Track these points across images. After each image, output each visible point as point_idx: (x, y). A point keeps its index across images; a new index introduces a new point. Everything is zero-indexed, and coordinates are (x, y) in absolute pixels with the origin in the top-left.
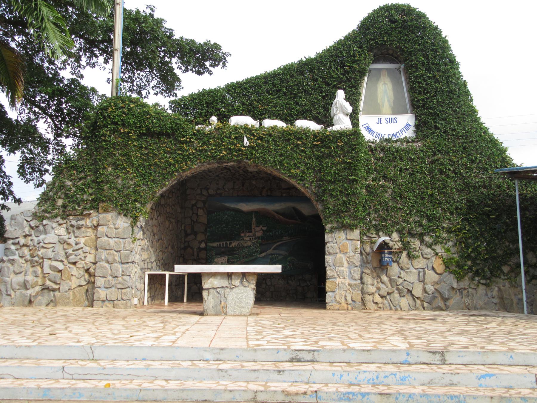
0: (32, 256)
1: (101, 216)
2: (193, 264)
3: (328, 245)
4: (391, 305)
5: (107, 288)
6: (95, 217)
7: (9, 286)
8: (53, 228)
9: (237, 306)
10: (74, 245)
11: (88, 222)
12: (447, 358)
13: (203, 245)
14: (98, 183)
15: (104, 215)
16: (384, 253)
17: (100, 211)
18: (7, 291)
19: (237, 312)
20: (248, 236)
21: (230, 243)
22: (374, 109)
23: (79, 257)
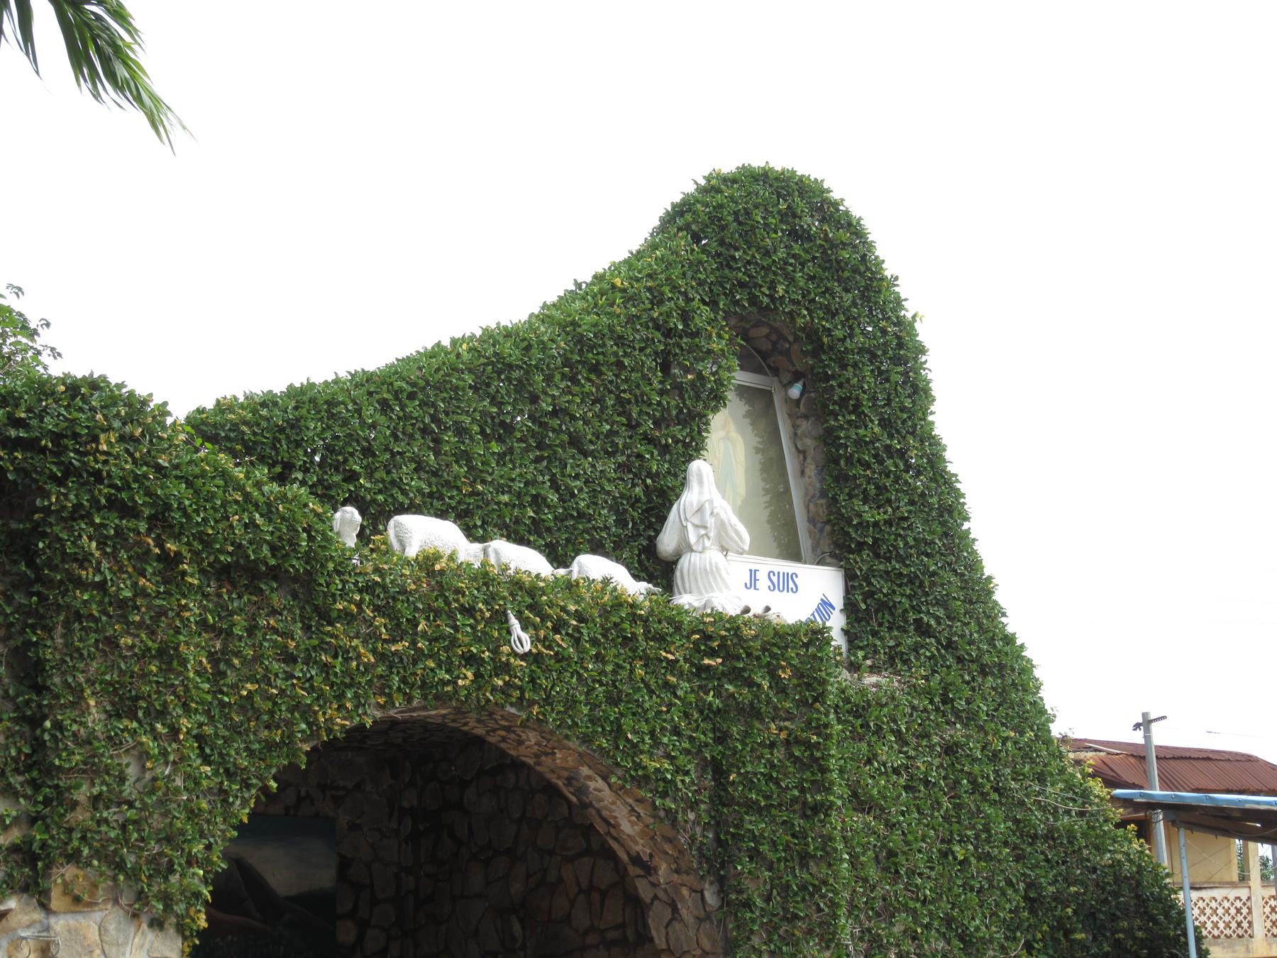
1: (59, 924)
17: (54, 904)
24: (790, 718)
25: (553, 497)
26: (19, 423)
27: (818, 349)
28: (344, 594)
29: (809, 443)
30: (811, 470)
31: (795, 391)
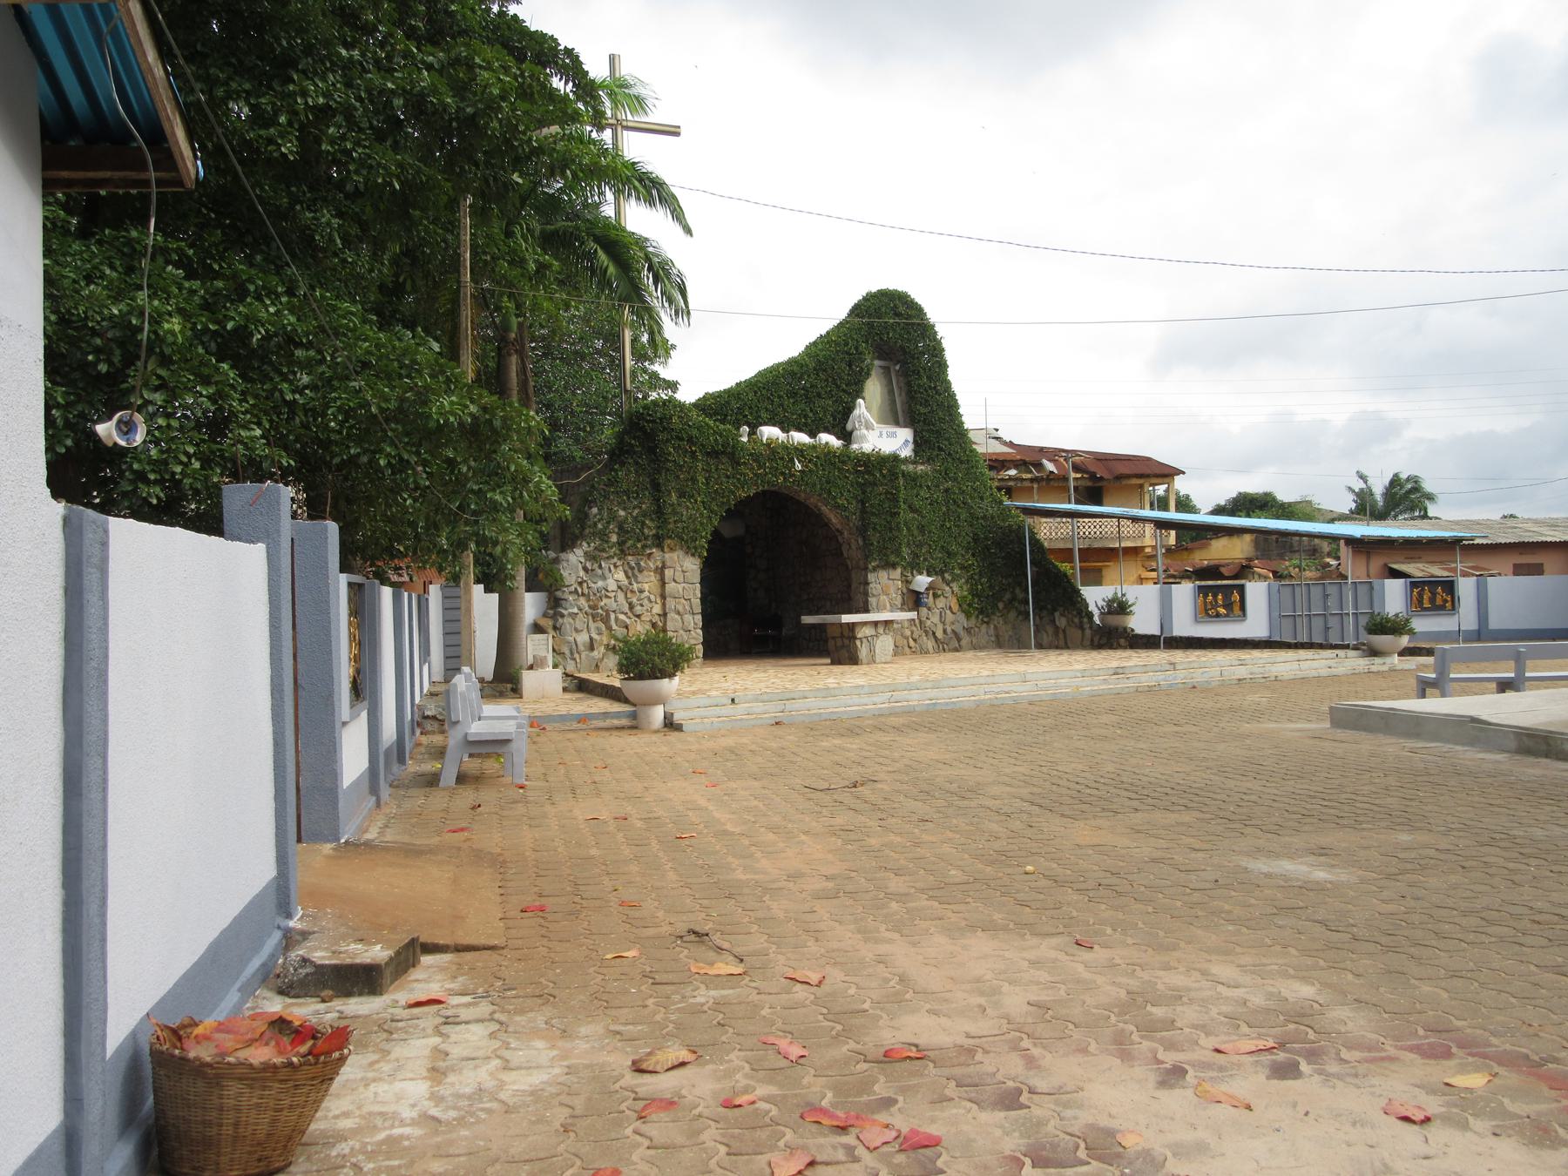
0: (593, 607)
1: (667, 556)
3: (871, 585)
14: (659, 513)
15: (671, 555)
24: (886, 485)
25: (811, 415)
26: (650, 415)
27: (905, 352)
28: (744, 457)
29: (902, 385)
30: (903, 394)
31: (897, 367)
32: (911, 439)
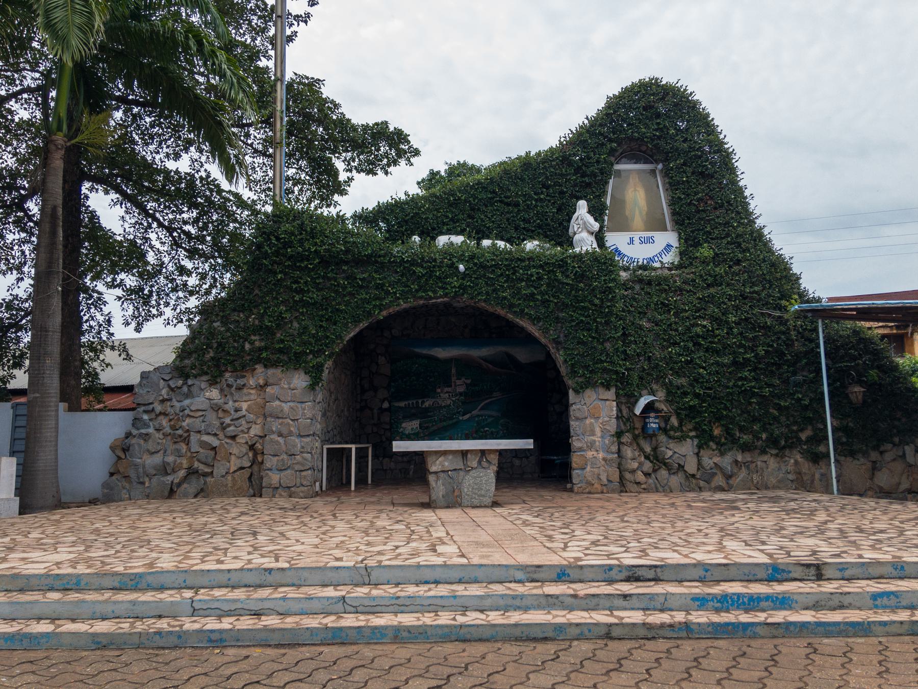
0: (174, 428)
2: (424, 440)
4: (658, 485)
5: (281, 470)
6: (260, 374)
7: (141, 470)
8: (202, 390)
9: (475, 494)
10: (232, 412)
11: (252, 382)
12: (823, 572)
13: (386, 405)
16: (649, 417)
18: (138, 478)
19: (476, 502)
20: (447, 392)
21: (423, 402)
22: (623, 226)
23: (240, 429)
32: (675, 244)
